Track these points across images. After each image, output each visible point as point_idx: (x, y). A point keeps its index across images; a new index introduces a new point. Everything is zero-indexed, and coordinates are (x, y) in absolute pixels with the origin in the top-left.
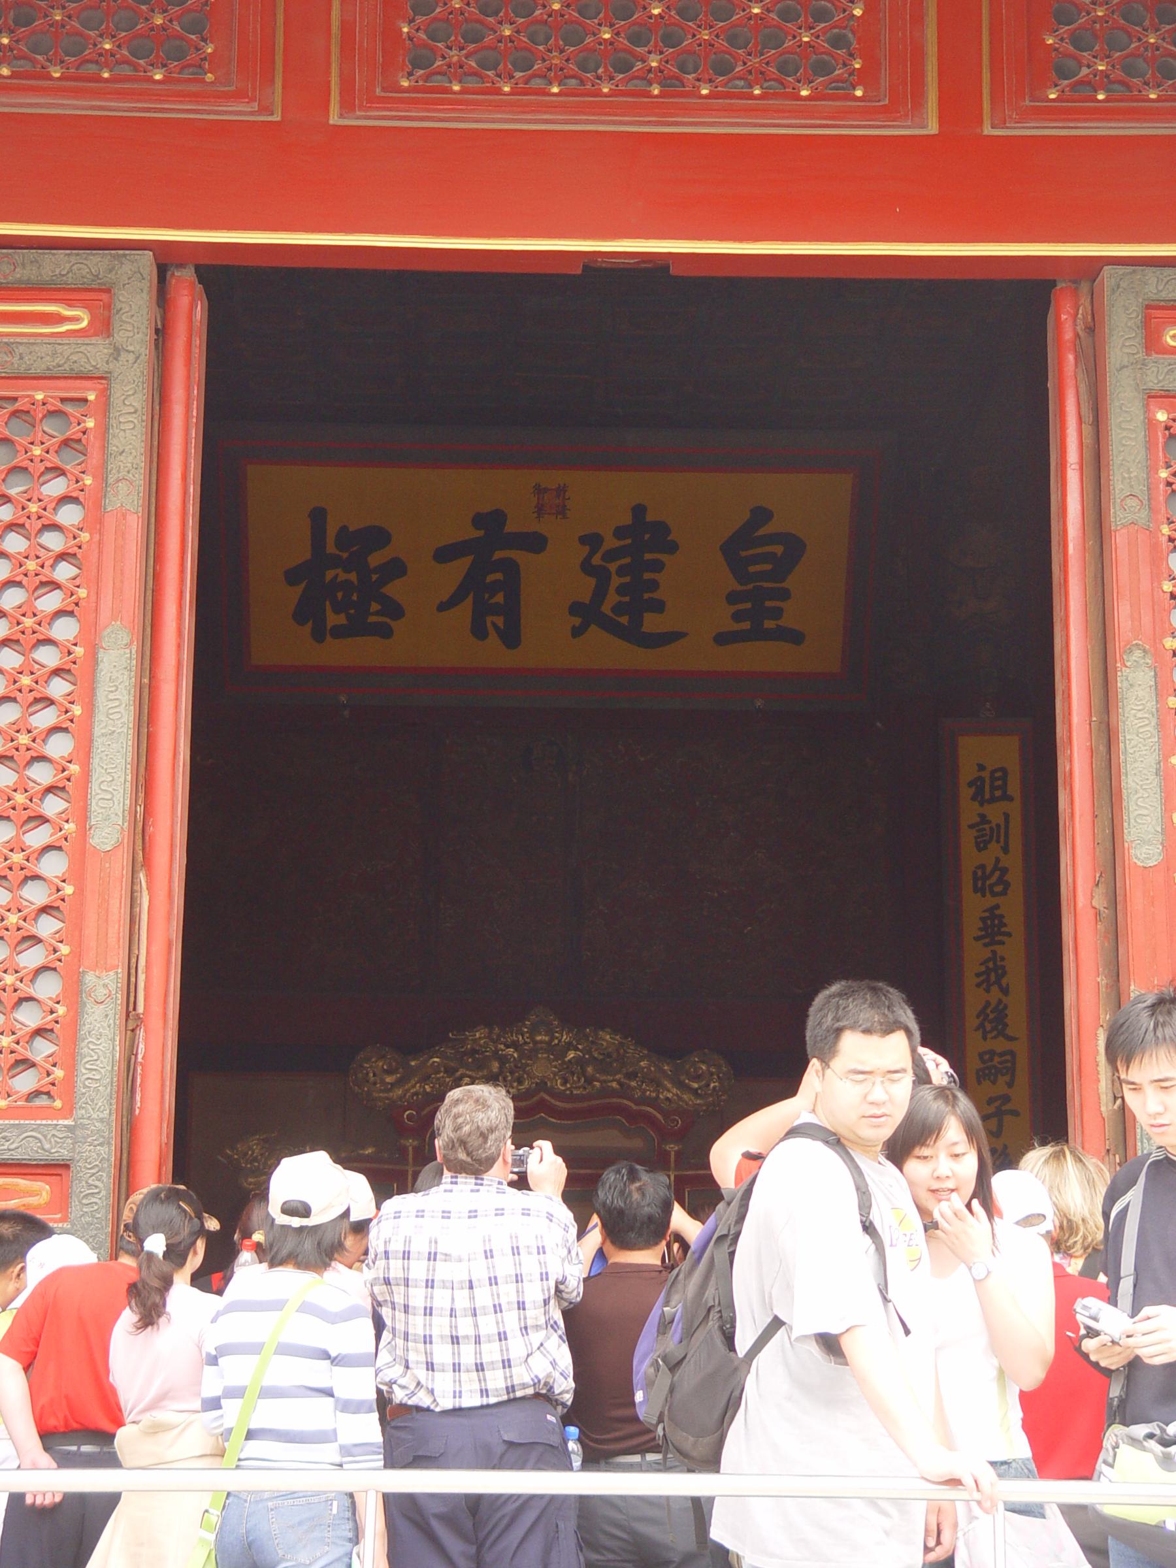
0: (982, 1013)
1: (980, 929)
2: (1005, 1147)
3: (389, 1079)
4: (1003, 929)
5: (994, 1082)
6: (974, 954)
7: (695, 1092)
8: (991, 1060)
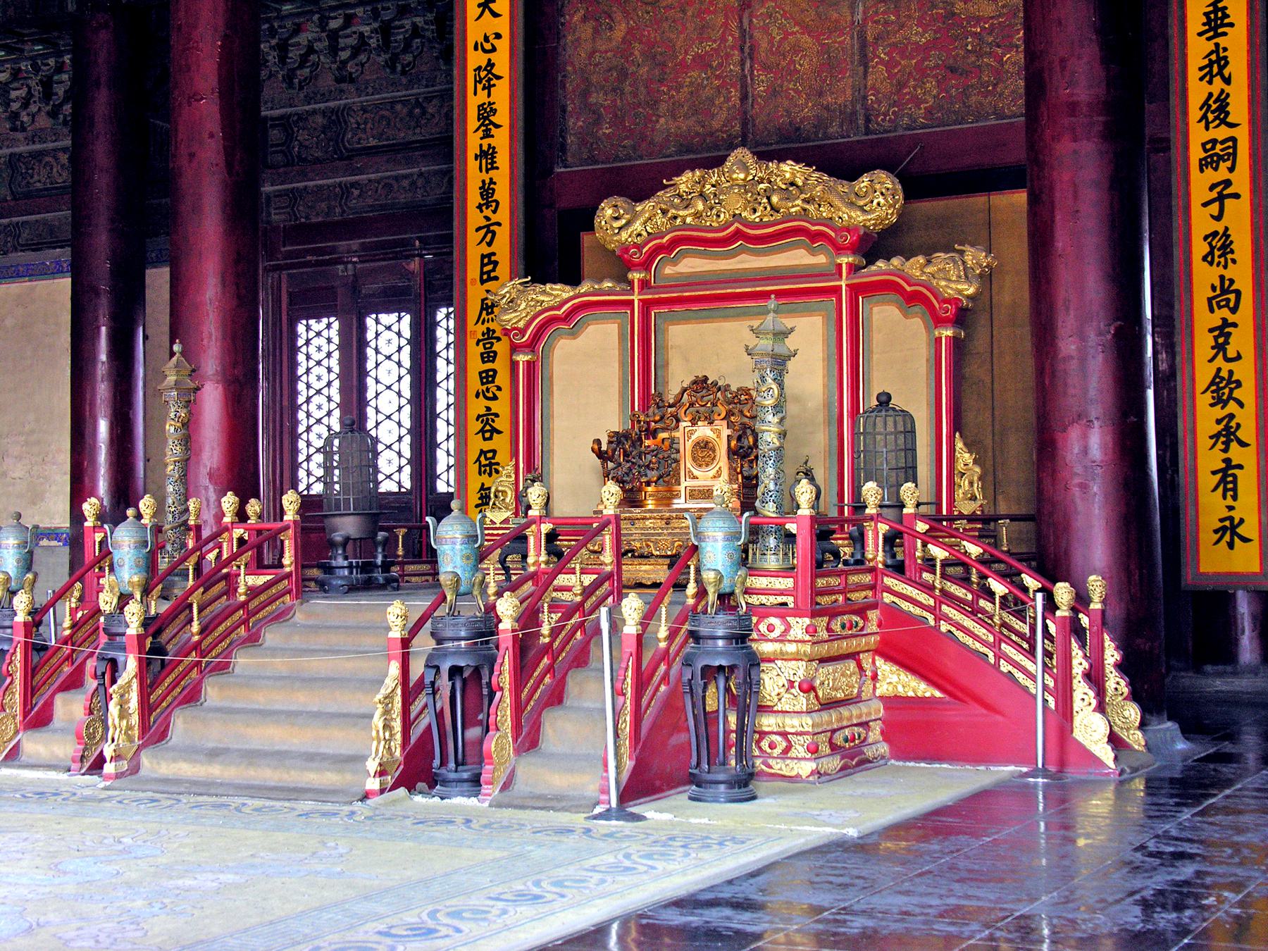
0: (1206, 103)
1: (1204, 24)
2: (1227, 229)
3: (617, 224)
4: (1226, 21)
5: (1216, 169)
6: (1198, 49)
7: (861, 208)
8: (1213, 148)
